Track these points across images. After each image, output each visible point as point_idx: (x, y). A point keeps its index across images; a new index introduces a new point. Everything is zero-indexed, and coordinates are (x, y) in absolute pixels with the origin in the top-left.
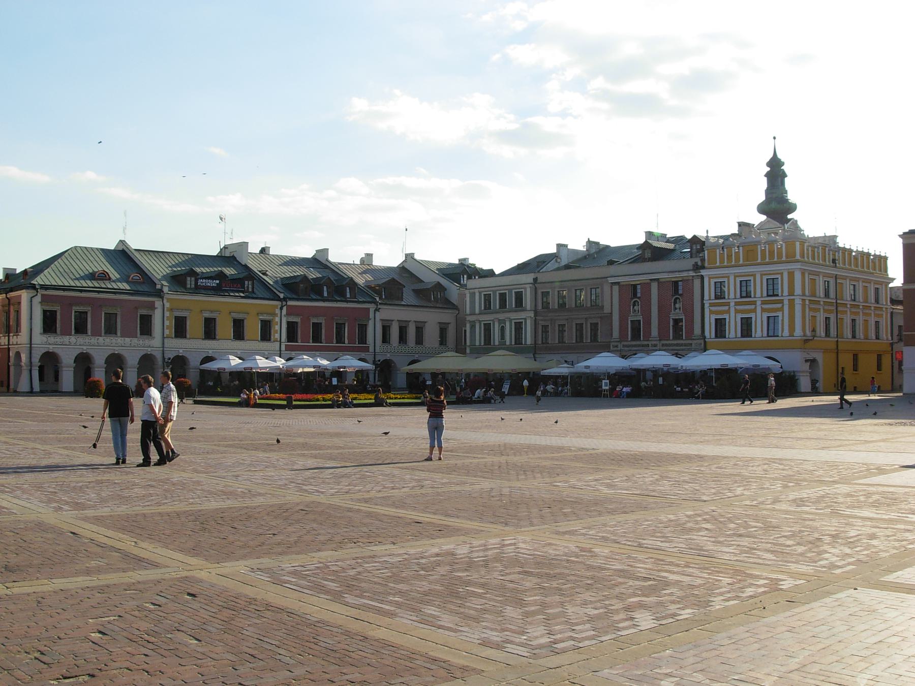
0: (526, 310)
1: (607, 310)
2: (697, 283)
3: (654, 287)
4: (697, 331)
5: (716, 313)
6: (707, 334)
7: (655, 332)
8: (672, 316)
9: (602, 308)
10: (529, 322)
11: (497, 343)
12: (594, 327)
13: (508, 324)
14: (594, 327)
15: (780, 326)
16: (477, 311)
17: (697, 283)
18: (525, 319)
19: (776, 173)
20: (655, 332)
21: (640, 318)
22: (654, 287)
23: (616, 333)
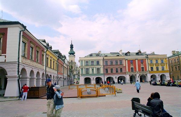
0: (100, 65)
1: (124, 65)
2: (147, 60)
3: (137, 61)
4: (148, 70)
5: (151, 66)
6: (149, 70)
7: (137, 70)
8: (141, 67)
9: (123, 65)
10: (102, 68)
11: (91, 73)
12: (121, 69)
13: (95, 68)
14: (121, 69)
15: (168, 67)
16: (84, 65)
17: (147, 60)
18: (101, 67)
19: (72, 47)
20: (137, 70)
21: (133, 67)
22: (137, 61)
23: (127, 70)
